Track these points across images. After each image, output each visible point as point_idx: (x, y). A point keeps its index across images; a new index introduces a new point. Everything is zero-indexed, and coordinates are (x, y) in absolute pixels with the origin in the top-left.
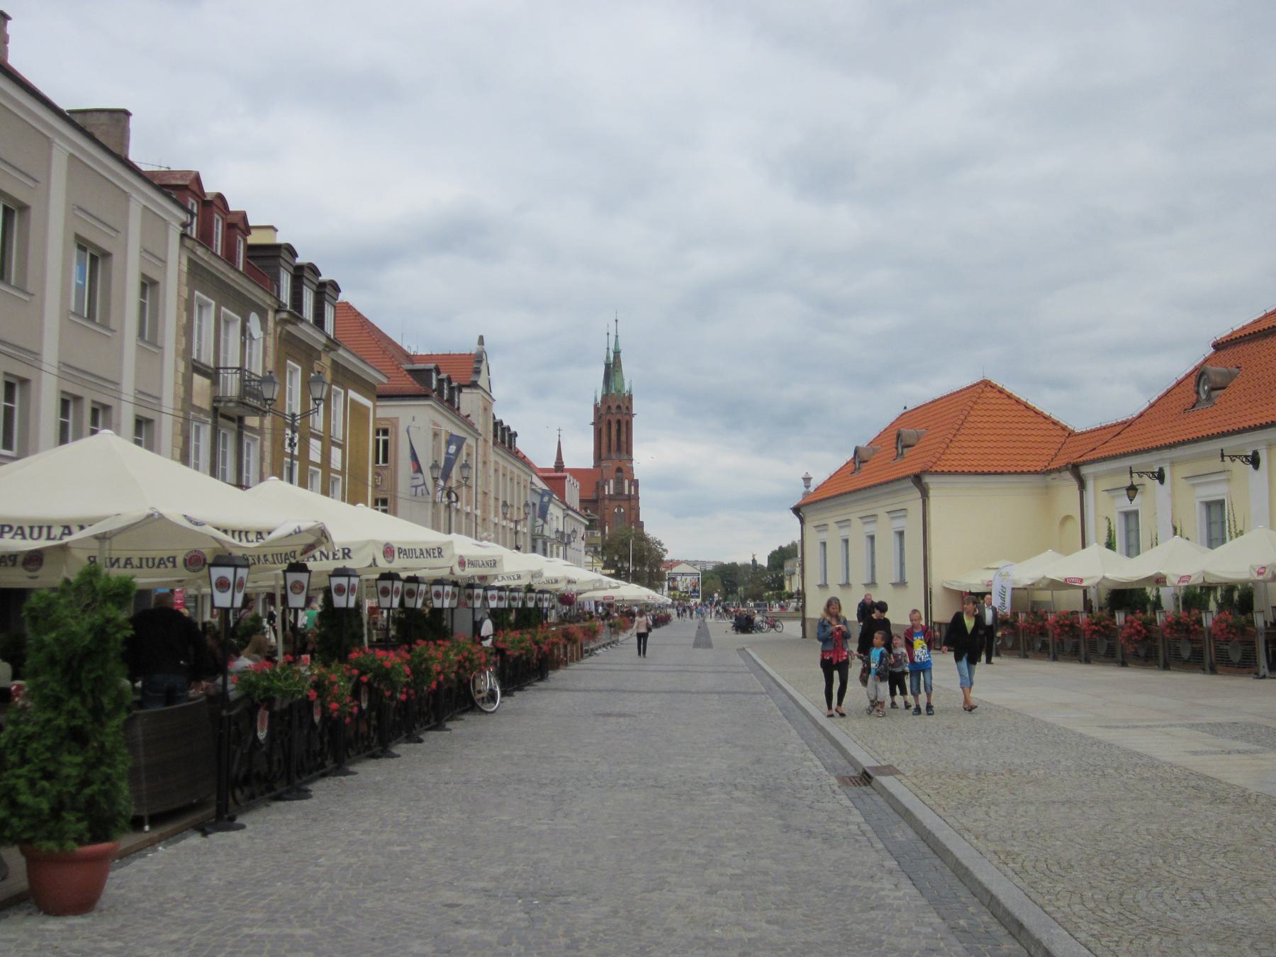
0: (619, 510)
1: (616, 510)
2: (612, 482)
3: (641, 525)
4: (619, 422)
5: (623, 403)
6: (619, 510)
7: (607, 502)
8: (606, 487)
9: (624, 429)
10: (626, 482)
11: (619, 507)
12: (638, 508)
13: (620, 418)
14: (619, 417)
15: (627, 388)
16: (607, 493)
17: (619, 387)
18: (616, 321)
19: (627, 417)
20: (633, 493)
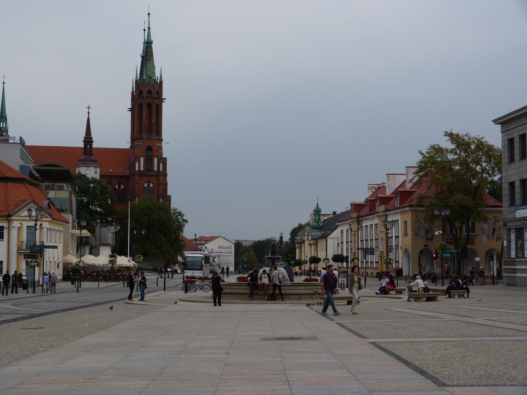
0: (149, 185)
1: (146, 185)
2: (142, 159)
3: (168, 199)
4: (149, 105)
5: (154, 88)
6: (149, 185)
7: (137, 177)
8: (137, 164)
9: (154, 112)
10: (156, 160)
11: (149, 182)
12: (166, 184)
13: (151, 102)
14: (150, 101)
15: (157, 74)
16: (137, 169)
17: (150, 74)
18: (149, 14)
19: (158, 102)
20: (161, 169)
